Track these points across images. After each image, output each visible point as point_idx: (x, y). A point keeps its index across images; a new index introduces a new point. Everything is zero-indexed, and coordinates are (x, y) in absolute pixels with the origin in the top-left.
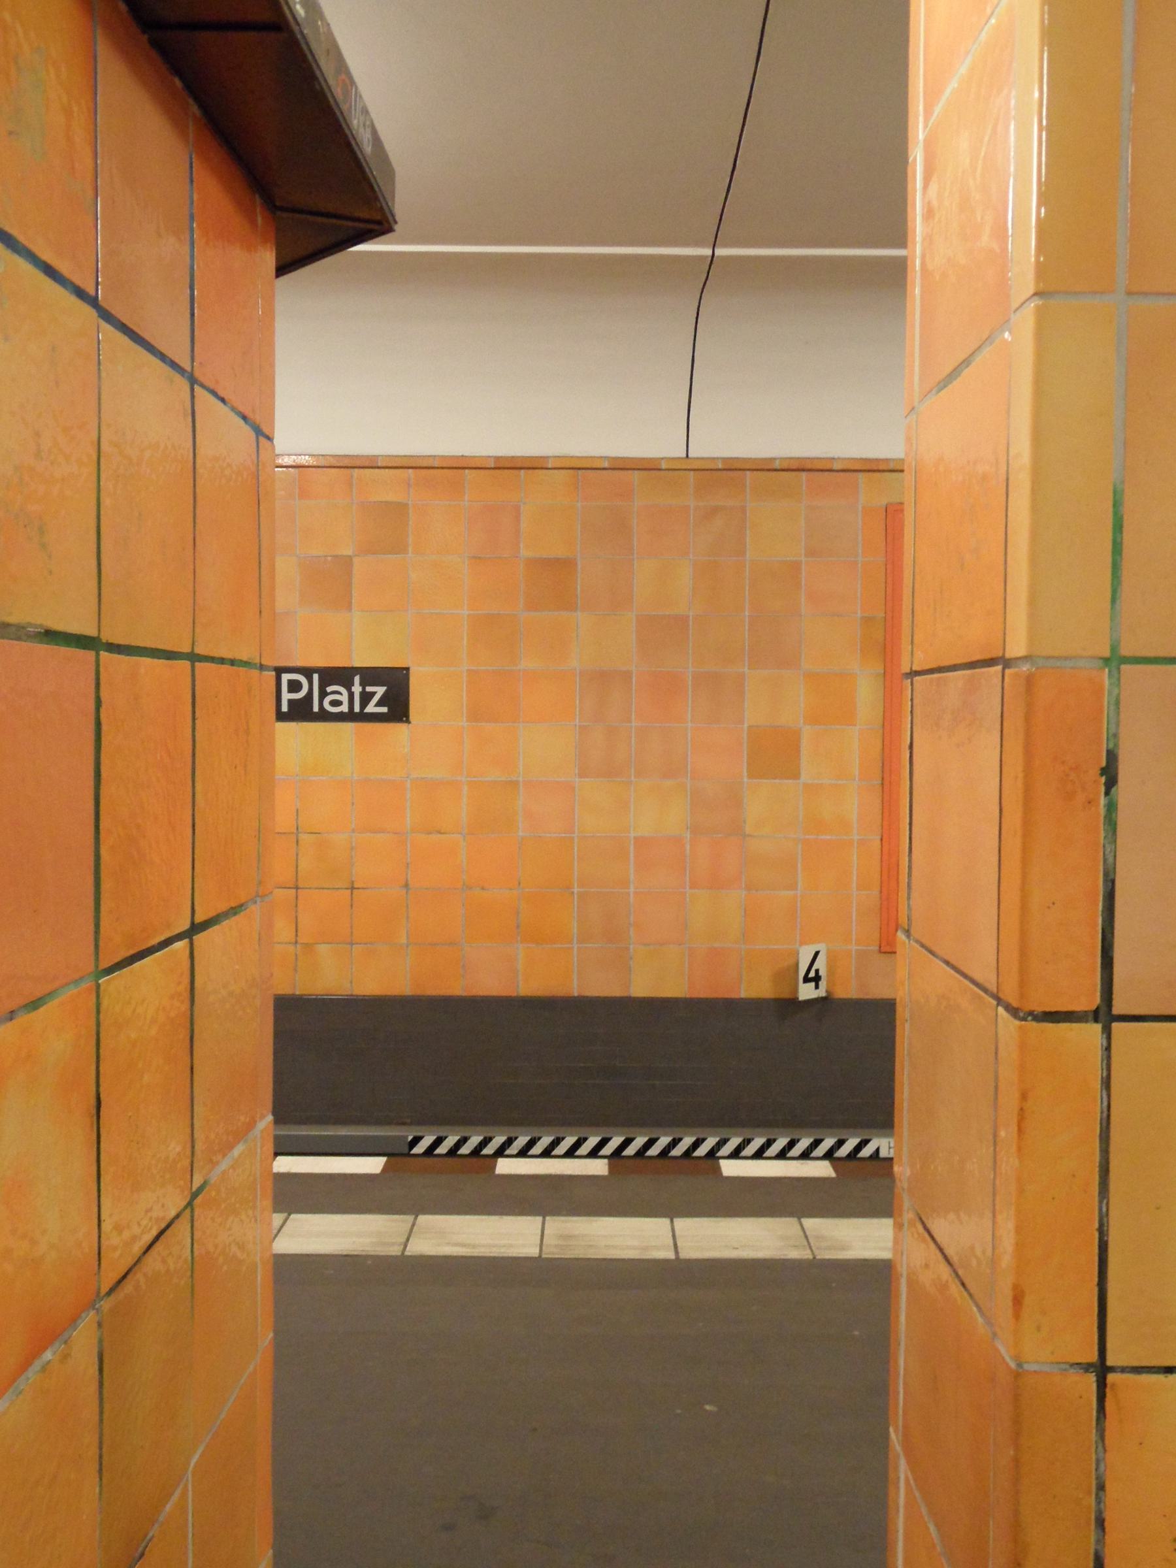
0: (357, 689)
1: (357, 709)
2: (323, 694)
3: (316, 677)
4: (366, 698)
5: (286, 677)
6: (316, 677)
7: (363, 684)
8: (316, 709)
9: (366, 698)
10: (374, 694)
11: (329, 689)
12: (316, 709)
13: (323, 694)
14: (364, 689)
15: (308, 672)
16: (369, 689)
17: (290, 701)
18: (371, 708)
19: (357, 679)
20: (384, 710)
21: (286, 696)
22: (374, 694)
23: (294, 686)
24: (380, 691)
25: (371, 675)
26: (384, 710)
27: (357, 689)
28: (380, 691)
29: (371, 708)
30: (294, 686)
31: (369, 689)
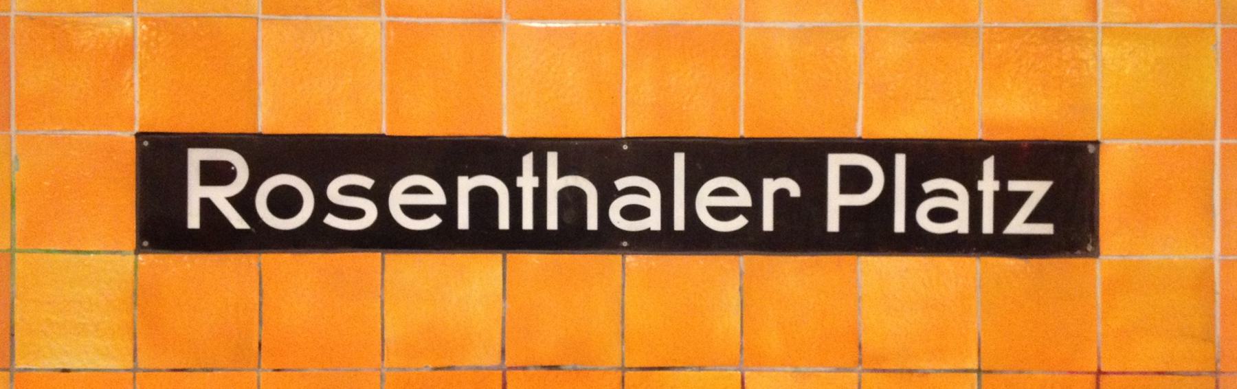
0: (988, 185)
1: (988, 227)
2: (915, 197)
3: (900, 160)
4: (1007, 204)
5: (835, 162)
6: (900, 160)
7: (1002, 175)
8: (900, 226)
9: (1007, 204)
10: (1025, 196)
11: (929, 186)
12: (900, 226)
13: (915, 197)
14: (1004, 186)
15: (883, 150)
16: (1015, 186)
17: (844, 210)
18: (1018, 226)
19: (989, 165)
20: (1046, 229)
21: (836, 200)
22: (1025, 196)
23: (855, 180)
24: (1039, 189)
25: (1018, 158)
26: (1046, 229)
27: (988, 185)
28: (1039, 189)
29: (1018, 226)
30: (855, 180)
31: (1015, 186)
